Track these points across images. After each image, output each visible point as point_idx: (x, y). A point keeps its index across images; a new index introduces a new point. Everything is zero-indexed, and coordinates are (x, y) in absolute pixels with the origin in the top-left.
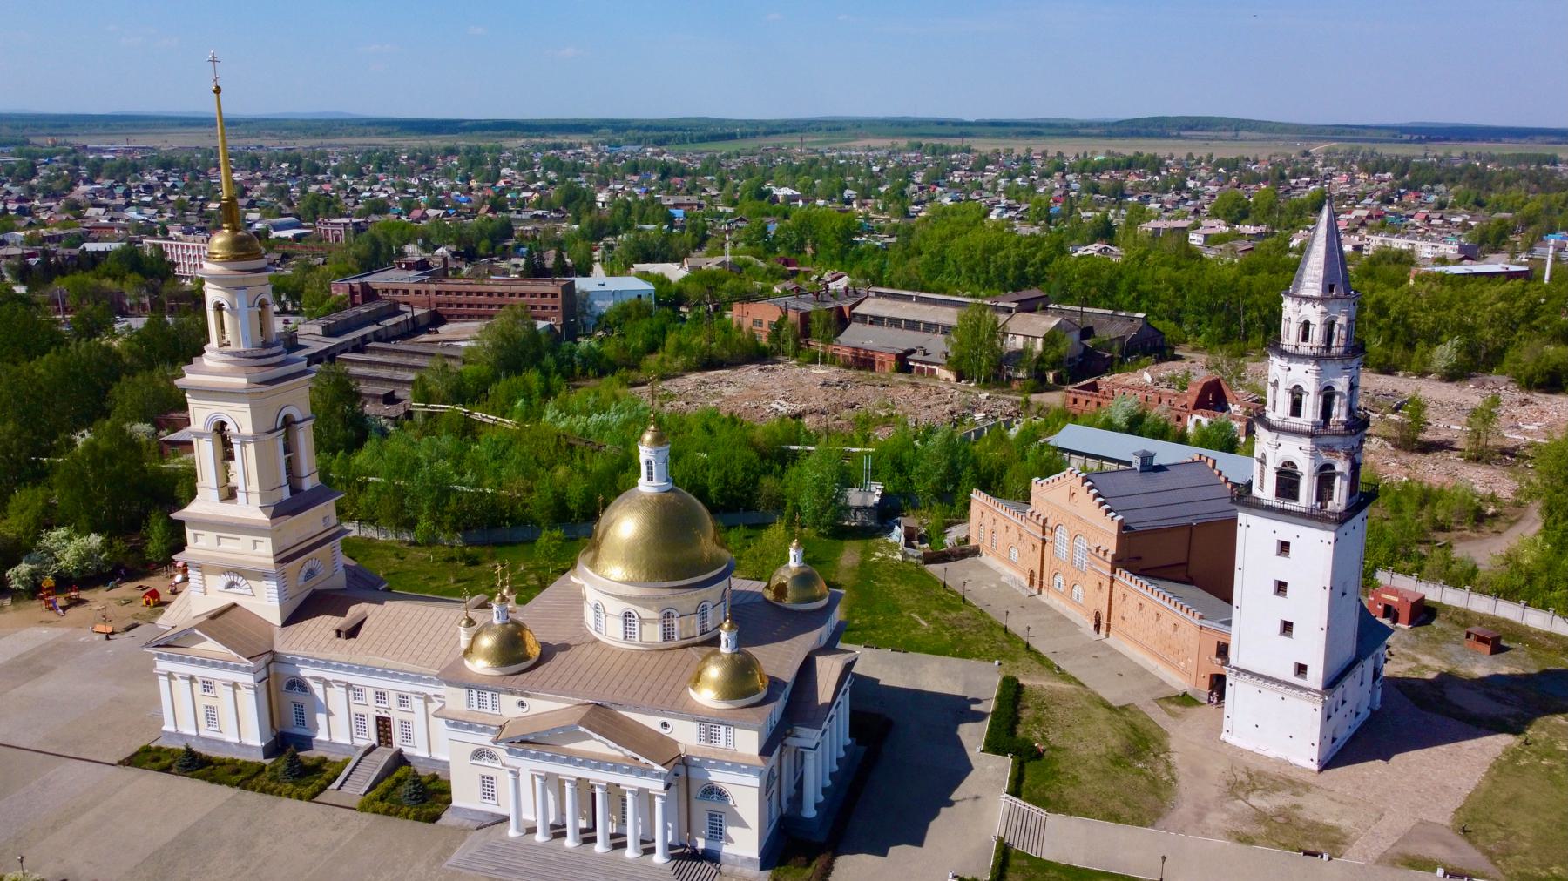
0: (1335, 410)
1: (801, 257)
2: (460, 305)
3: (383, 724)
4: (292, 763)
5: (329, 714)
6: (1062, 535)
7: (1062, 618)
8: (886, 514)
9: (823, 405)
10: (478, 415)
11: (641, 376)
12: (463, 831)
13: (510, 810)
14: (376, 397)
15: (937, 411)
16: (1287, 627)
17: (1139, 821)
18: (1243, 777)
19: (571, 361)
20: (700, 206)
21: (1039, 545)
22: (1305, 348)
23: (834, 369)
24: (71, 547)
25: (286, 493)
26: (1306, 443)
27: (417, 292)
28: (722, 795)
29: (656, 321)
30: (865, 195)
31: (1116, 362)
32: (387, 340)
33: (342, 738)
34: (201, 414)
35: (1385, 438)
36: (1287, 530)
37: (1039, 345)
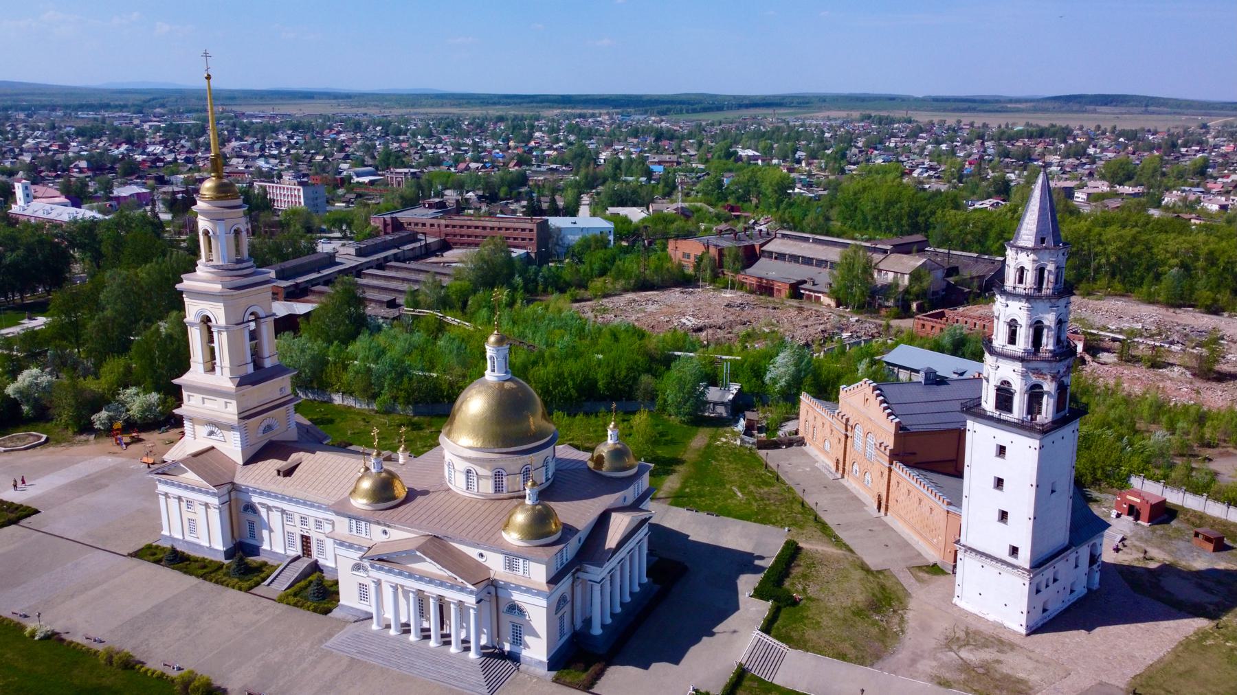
0: (1044, 341)
1: (746, 205)
2: (462, 236)
3: (306, 540)
4: (243, 564)
5: (271, 531)
6: (858, 432)
7: (855, 498)
8: (738, 407)
9: (721, 321)
10: (449, 318)
11: (588, 294)
12: (345, 622)
13: (373, 610)
14: (380, 302)
15: (811, 330)
16: (1004, 516)
17: (861, 661)
18: (962, 635)
19: (535, 281)
20: (679, 163)
21: (843, 439)
22: (1020, 289)
23: (740, 293)
24: (137, 401)
25: (250, 369)
26: (1018, 366)
27: (432, 225)
28: (521, 612)
29: (609, 252)
30: (813, 156)
31: (972, 296)
32: (404, 261)
33: (279, 549)
34: (193, 310)
35: (1187, 368)
37: (906, 280)
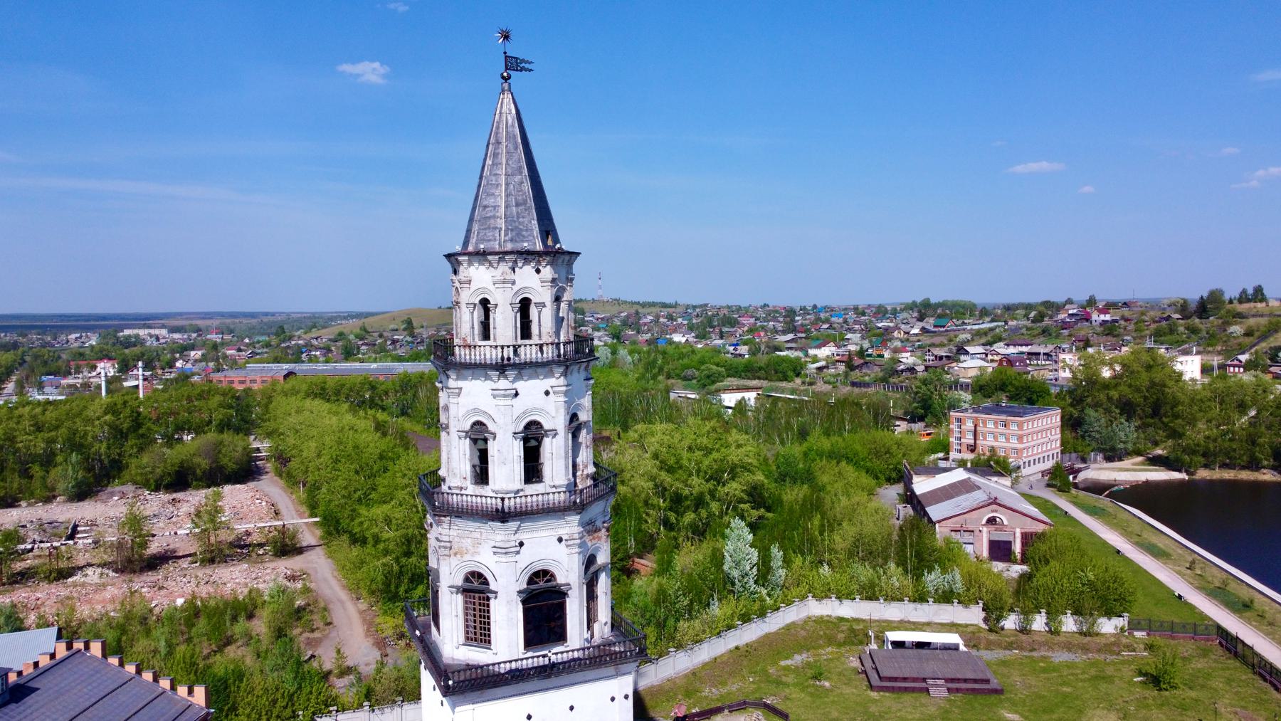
22: (529, 353)
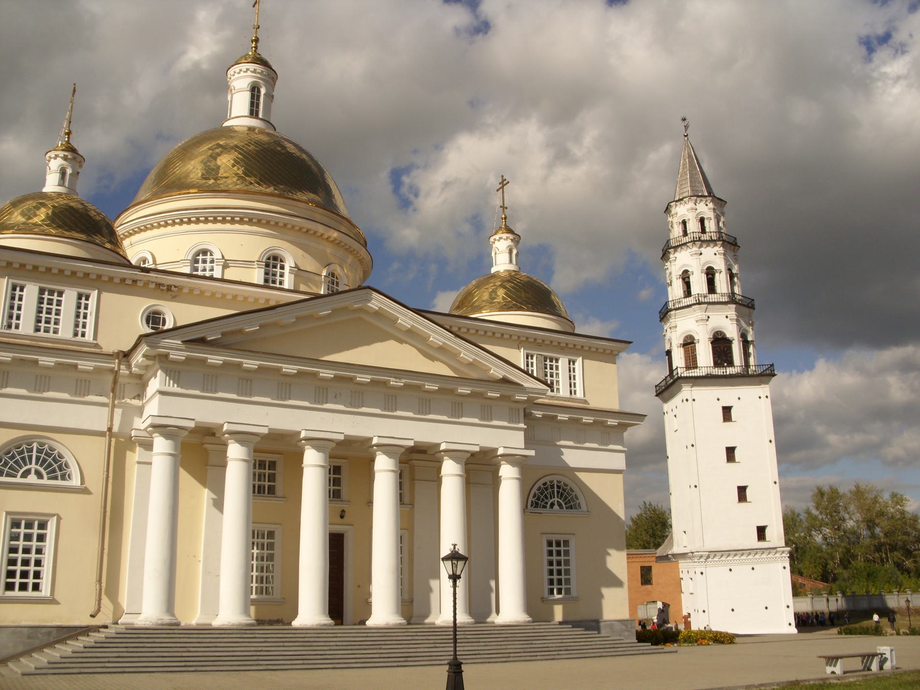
16: (742, 492)
36: (728, 394)
